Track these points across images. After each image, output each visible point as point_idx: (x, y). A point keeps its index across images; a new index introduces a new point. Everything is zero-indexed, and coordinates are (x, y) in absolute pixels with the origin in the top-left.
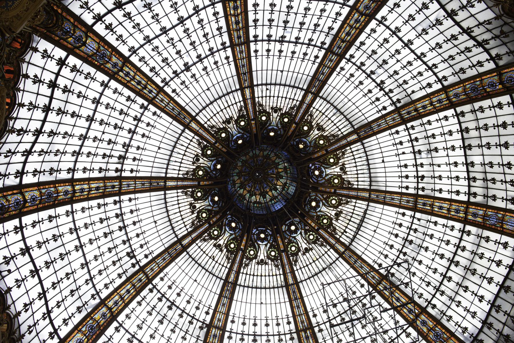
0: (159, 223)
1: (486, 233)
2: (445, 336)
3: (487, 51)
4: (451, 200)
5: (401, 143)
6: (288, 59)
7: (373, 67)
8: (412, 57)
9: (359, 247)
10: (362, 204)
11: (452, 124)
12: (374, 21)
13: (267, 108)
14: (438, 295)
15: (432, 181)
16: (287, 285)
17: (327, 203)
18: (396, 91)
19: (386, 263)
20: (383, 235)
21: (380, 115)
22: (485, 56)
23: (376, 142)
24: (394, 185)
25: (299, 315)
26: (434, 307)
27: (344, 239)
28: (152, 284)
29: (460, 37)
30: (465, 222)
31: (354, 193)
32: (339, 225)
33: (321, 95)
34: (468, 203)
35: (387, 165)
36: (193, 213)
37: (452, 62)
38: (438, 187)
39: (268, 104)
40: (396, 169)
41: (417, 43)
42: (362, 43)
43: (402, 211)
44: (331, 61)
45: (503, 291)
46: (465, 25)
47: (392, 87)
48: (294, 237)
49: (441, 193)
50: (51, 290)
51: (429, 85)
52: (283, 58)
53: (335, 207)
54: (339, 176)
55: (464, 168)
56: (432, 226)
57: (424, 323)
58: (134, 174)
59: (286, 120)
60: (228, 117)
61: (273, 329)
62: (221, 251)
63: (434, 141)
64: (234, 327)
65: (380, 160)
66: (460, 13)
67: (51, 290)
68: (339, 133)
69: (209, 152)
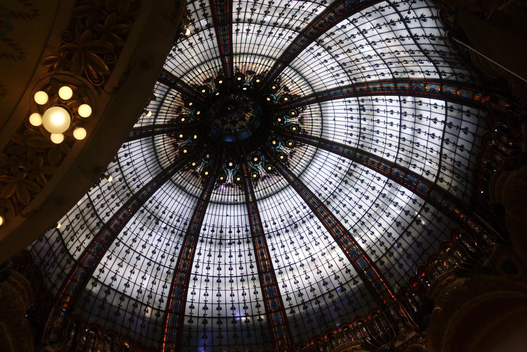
0: (147, 160)
2: (359, 253)
9: (306, 179)
15: (371, 142)
16: (247, 203)
17: (285, 143)
24: (339, 139)
25: (255, 225)
33: (290, 64)
35: (336, 123)
36: (175, 150)
38: (374, 147)
42: (333, 34)
48: (256, 167)
49: (375, 151)
51: (383, 74)
53: (291, 147)
54: (296, 125)
56: (364, 173)
59: (258, 81)
60: (208, 77)
62: (198, 177)
63: (378, 114)
65: (332, 118)
68: (302, 93)
69: (191, 104)
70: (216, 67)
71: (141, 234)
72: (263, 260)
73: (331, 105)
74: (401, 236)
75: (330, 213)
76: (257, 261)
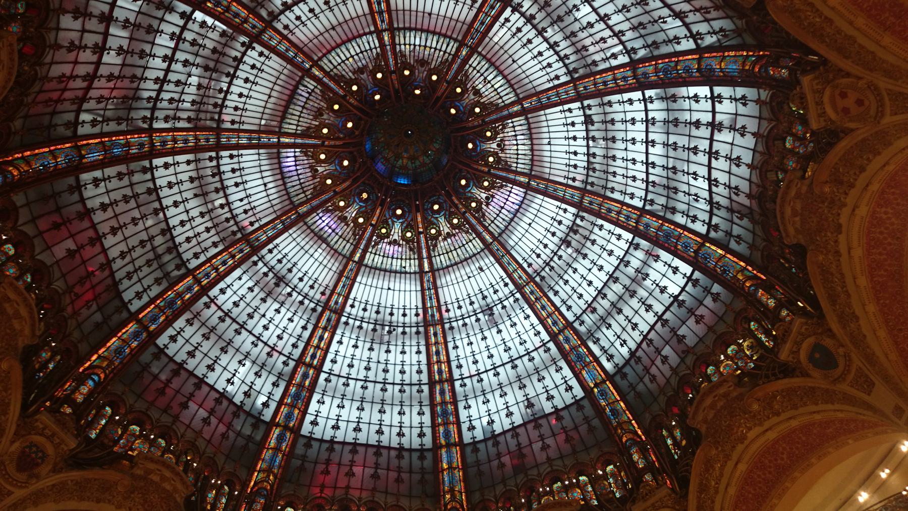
1: (562, 363)
3: (711, 214)
4: (557, 309)
5: (560, 223)
6: (530, 55)
7: (597, 134)
8: (641, 157)
9: (442, 281)
10: (478, 244)
11: (619, 247)
12: (640, 93)
13: (471, 83)
14: (475, 379)
15: (557, 279)
18: (597, 174)
19: (454, 313)
20: (472, 286)
21: (565, 181)
22: (706, 217)
23: (539, 202)
26: (463, 385)
27: (437, 261)
28: (217, 154)
29: (701, 180)
30: (553, 337)
31: (480, 229)
32: (442, 245)
33: (529, 116)
34: (569, 325)
35: (531, 230)
36: (315, 118)
37: (672, 195)
38: (557, 288)
39: (474, 79)
40: (535, 241)
41: (658, 150)
42: (610, 104)
43: (507, 280)
44: (567, 92)
45: (533, 424)
46: (715, 174)
47: (597, 167)
50: (103, 80)
51: (632, 196)
52: (526, 50)
55: (594, 294)
57: (442, 392)
58: (285, 32)
61: (303, 286)
62: (314, 177)
64: (269, 257)
65: (529, 221)
66: (722, 160)
67: (103, 80)
68: (515, 165)
70: (445, 52)
71: (187, 185)
72: (318, 347)
73: (539, 202)
74: (524, 424)
75: (446, 343)
76: (308, 343)
